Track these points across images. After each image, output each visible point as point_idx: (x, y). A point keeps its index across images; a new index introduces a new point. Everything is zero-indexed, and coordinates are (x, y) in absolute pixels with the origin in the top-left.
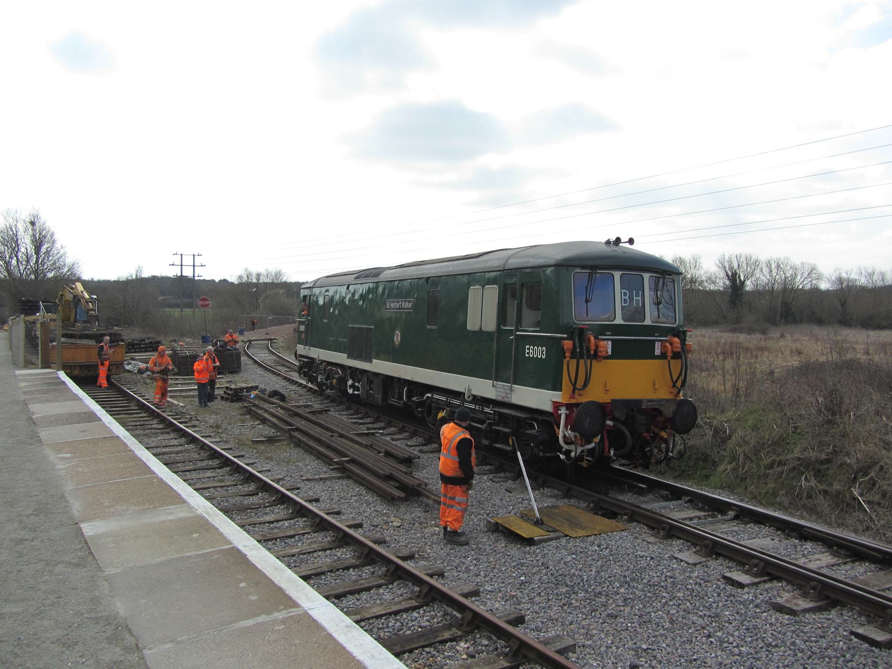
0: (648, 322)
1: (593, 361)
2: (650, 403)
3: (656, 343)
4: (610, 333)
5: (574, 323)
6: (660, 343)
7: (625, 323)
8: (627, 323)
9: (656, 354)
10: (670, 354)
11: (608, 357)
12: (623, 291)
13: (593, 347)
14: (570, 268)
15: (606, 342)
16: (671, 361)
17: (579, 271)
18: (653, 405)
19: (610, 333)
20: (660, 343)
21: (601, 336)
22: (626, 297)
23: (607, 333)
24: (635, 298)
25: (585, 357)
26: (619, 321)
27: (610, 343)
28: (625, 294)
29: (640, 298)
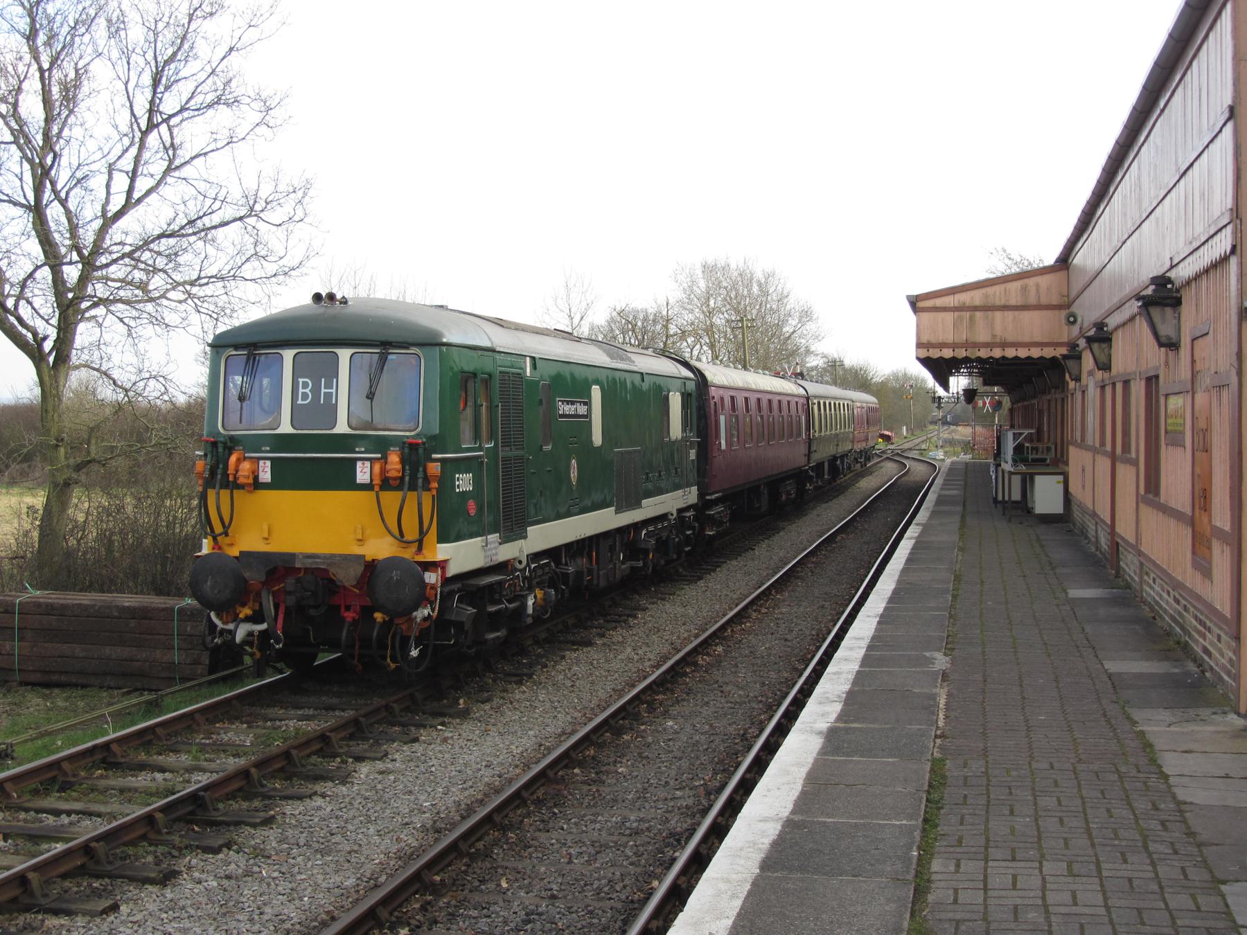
0: (342, 428)
1: (235, 491)
2: (310, 561)
3: (359, 464)
4: (268, 448)
5: (220, 433)
6: (368, 464)
7: (295, 432)
8: (299, 432)
9: (358, 481)
10: (377, 481)
11: (266, 486)
12: (301, 380)
13: (231, 470)
14: (219, 349)
15: (261, 463)
16: (380, 493)
17: (234, 353)
18: (316, 563)
19: (268, 448)
20: (368, 464)
21: (249, 452)
22: (307, 391)
23: (263, 449)
24: (323, 390)
25: (218, 486)
26: (286, 428)
27: (268, 463)
28: (305, 385)
29: (334, 391)
